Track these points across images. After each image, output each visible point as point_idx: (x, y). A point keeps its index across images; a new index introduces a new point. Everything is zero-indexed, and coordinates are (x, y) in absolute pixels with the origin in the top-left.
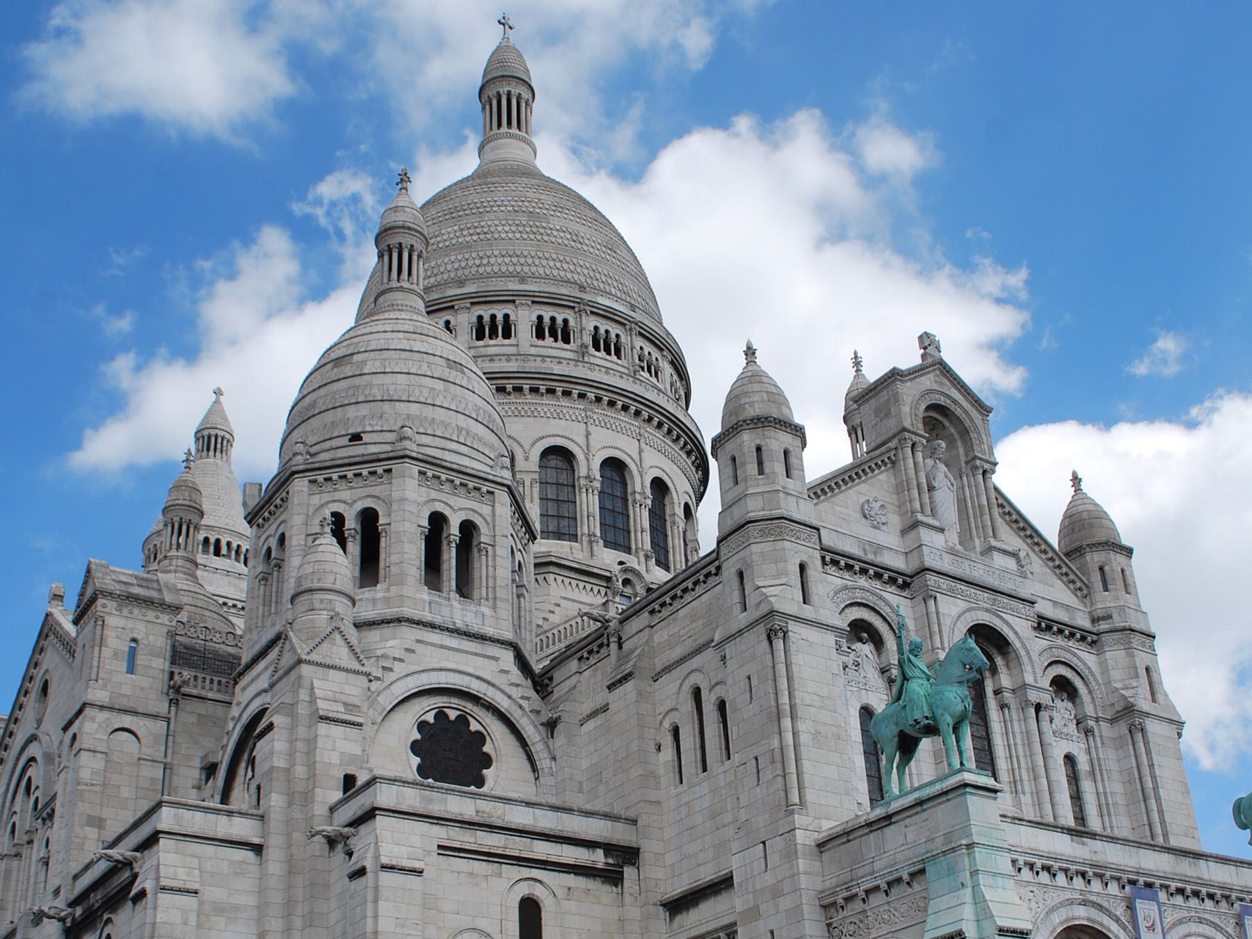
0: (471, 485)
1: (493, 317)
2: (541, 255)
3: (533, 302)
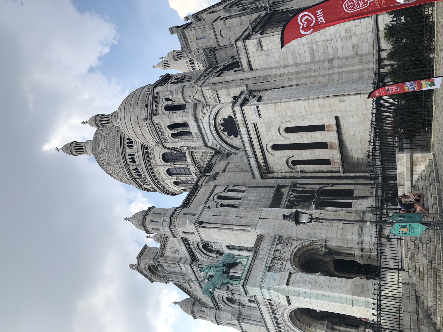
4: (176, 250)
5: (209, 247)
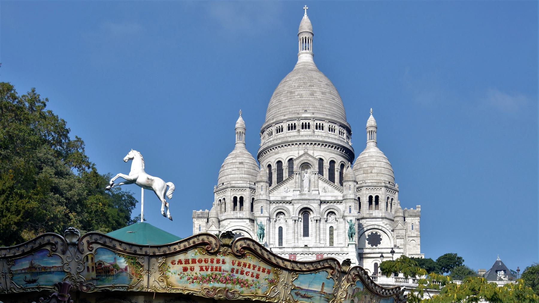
0: (241, 189)
1: (279, 127)
2: (291, 105)
3: (287, 121)
4: (326, 191)
5: (329, 215)
